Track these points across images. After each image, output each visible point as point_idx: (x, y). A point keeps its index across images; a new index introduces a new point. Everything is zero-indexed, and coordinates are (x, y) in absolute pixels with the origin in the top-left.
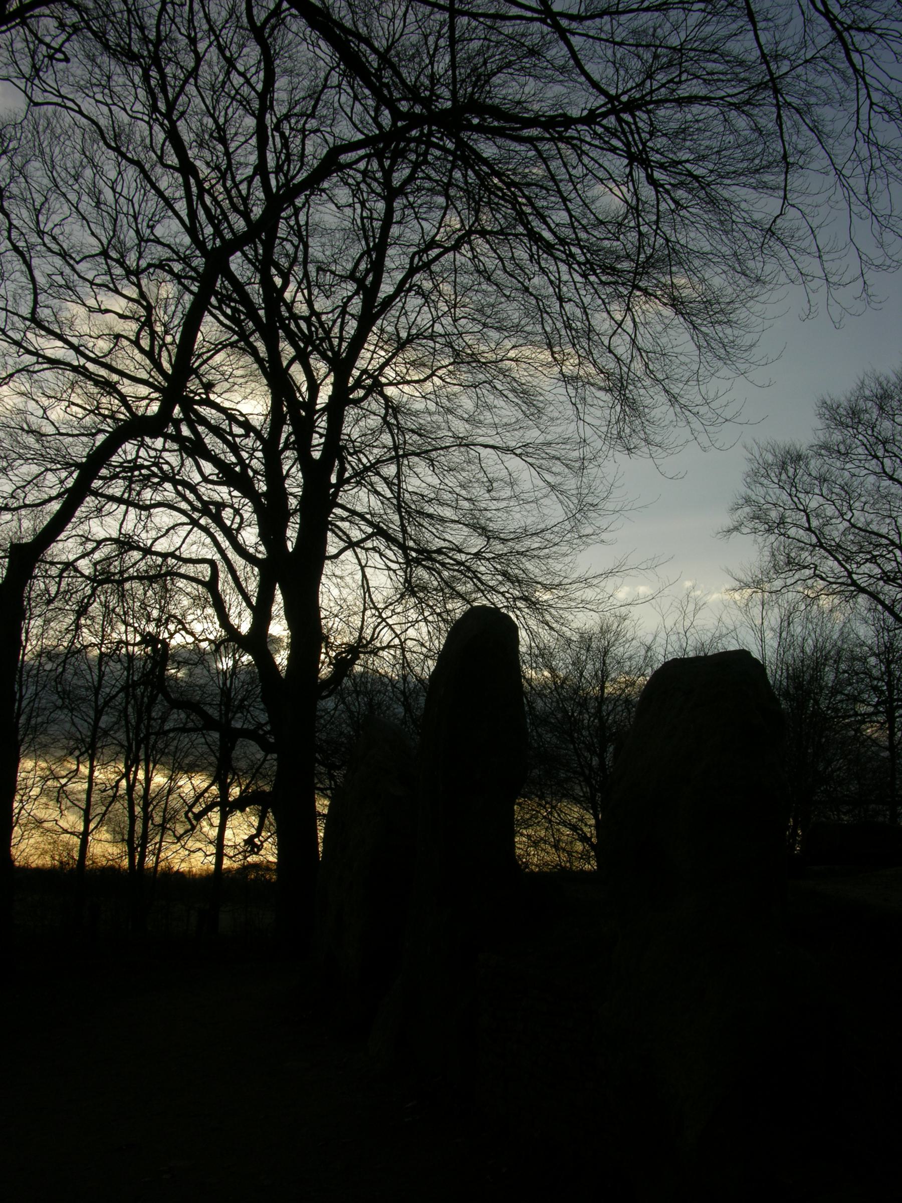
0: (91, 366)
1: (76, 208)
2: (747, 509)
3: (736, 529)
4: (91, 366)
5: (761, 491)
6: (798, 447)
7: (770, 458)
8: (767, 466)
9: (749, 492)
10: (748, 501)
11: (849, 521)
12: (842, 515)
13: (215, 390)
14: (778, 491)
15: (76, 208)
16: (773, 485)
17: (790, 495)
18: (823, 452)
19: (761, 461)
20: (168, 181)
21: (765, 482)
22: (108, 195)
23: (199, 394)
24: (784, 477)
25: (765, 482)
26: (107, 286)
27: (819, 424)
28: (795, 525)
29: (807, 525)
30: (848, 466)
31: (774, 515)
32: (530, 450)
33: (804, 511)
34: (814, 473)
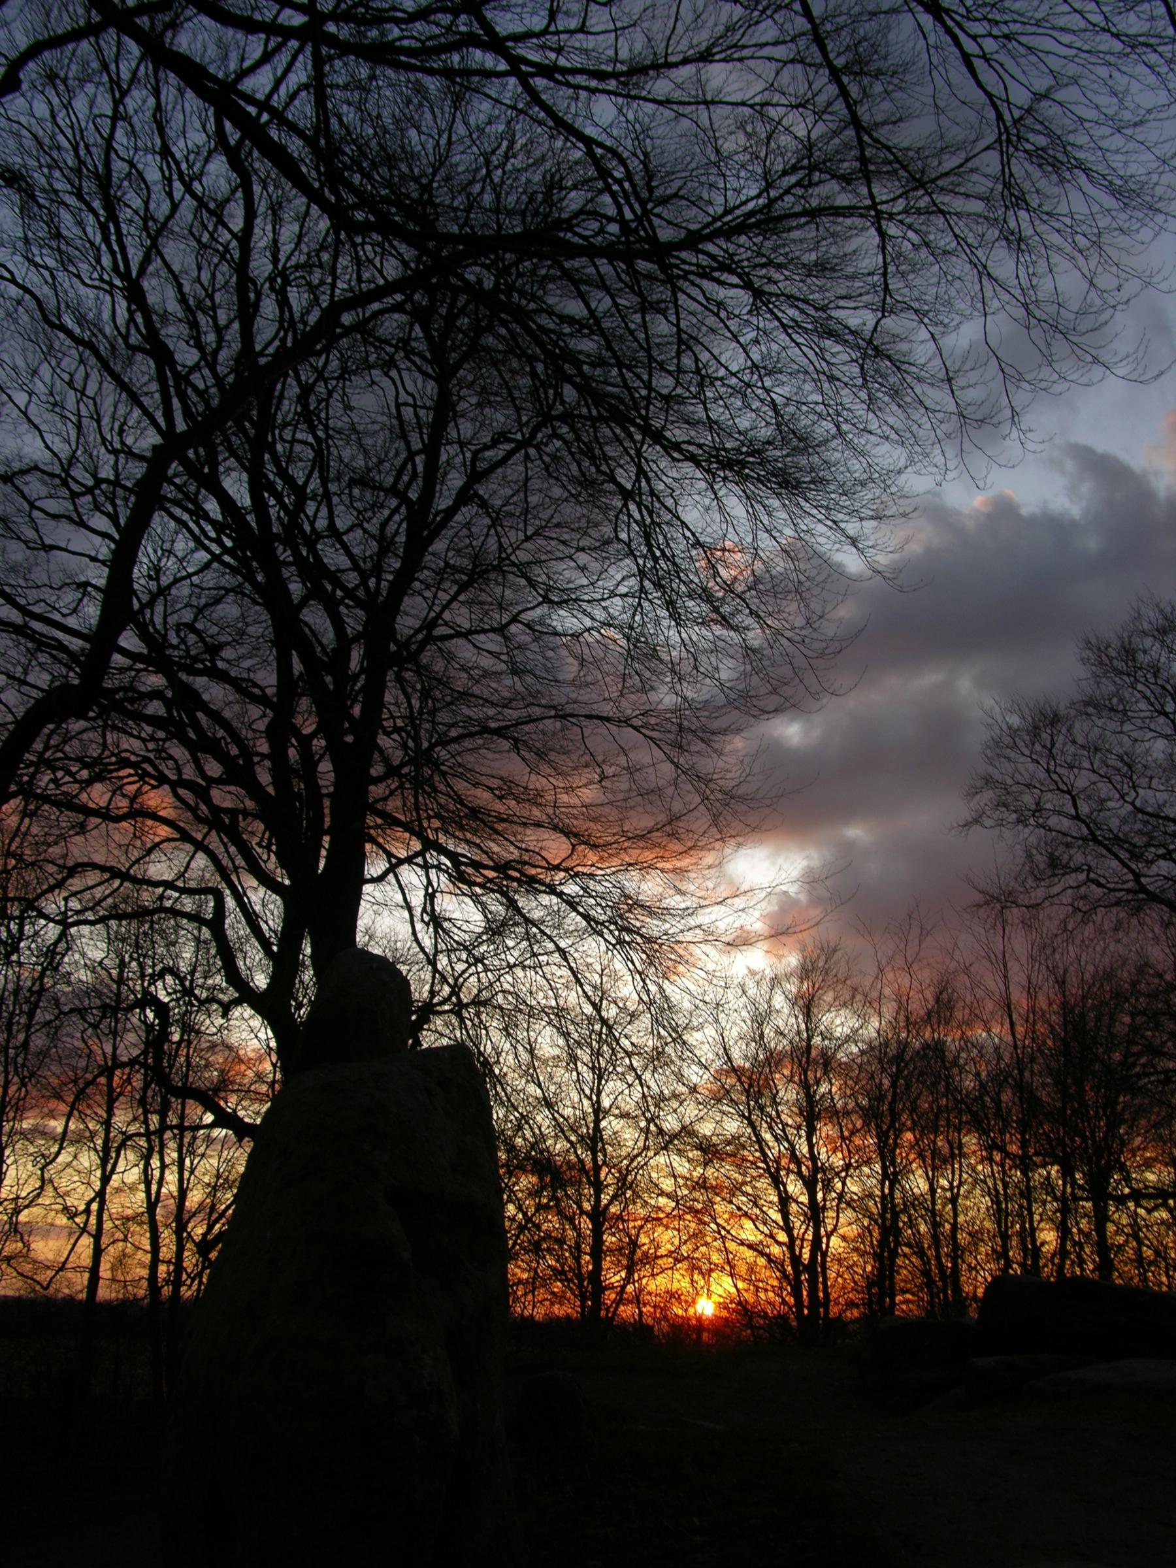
0: (36, 625)
1: (25, 414)
2: (988, 795)
3: (976, 821)
4: (36, 625)
5: (1008, 767)
6: (1054, 704)
7: (1015, 721)
8: (1013, 732)
9: (990, 769)
10: (988, 781)
11: (1132, 804)
12: (1122, 797)
13: (223, 654)
14: (1032, 767)
15: (25, 414)
16: (1023, 759)
17: (1048, 771)
18: (1090, 710)
19: (1004, 727)
20: (142, 371)
21: (1012, 755)
22: (71, 397)
23: (202, 662)
24: (1038, 747)
25: (1012, 755)
26: (69, 518)
27: (1083, 672)
28: (1059, 813)
29: (1073, 812)
30: (1127, 727)
31: (1028, 799)
32: (653, 721)
33: (1069, 792)
34: (1080, 740)
